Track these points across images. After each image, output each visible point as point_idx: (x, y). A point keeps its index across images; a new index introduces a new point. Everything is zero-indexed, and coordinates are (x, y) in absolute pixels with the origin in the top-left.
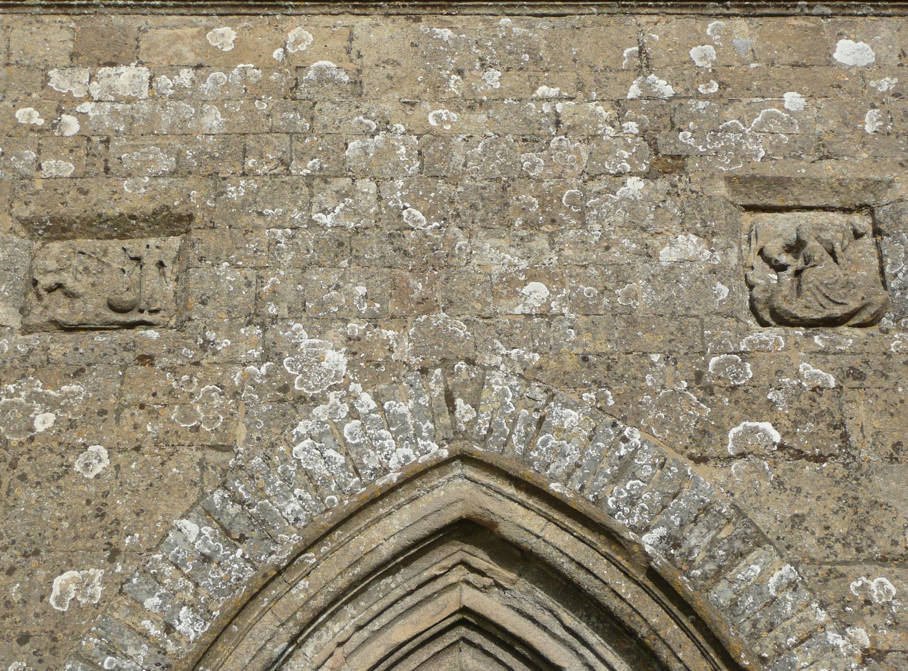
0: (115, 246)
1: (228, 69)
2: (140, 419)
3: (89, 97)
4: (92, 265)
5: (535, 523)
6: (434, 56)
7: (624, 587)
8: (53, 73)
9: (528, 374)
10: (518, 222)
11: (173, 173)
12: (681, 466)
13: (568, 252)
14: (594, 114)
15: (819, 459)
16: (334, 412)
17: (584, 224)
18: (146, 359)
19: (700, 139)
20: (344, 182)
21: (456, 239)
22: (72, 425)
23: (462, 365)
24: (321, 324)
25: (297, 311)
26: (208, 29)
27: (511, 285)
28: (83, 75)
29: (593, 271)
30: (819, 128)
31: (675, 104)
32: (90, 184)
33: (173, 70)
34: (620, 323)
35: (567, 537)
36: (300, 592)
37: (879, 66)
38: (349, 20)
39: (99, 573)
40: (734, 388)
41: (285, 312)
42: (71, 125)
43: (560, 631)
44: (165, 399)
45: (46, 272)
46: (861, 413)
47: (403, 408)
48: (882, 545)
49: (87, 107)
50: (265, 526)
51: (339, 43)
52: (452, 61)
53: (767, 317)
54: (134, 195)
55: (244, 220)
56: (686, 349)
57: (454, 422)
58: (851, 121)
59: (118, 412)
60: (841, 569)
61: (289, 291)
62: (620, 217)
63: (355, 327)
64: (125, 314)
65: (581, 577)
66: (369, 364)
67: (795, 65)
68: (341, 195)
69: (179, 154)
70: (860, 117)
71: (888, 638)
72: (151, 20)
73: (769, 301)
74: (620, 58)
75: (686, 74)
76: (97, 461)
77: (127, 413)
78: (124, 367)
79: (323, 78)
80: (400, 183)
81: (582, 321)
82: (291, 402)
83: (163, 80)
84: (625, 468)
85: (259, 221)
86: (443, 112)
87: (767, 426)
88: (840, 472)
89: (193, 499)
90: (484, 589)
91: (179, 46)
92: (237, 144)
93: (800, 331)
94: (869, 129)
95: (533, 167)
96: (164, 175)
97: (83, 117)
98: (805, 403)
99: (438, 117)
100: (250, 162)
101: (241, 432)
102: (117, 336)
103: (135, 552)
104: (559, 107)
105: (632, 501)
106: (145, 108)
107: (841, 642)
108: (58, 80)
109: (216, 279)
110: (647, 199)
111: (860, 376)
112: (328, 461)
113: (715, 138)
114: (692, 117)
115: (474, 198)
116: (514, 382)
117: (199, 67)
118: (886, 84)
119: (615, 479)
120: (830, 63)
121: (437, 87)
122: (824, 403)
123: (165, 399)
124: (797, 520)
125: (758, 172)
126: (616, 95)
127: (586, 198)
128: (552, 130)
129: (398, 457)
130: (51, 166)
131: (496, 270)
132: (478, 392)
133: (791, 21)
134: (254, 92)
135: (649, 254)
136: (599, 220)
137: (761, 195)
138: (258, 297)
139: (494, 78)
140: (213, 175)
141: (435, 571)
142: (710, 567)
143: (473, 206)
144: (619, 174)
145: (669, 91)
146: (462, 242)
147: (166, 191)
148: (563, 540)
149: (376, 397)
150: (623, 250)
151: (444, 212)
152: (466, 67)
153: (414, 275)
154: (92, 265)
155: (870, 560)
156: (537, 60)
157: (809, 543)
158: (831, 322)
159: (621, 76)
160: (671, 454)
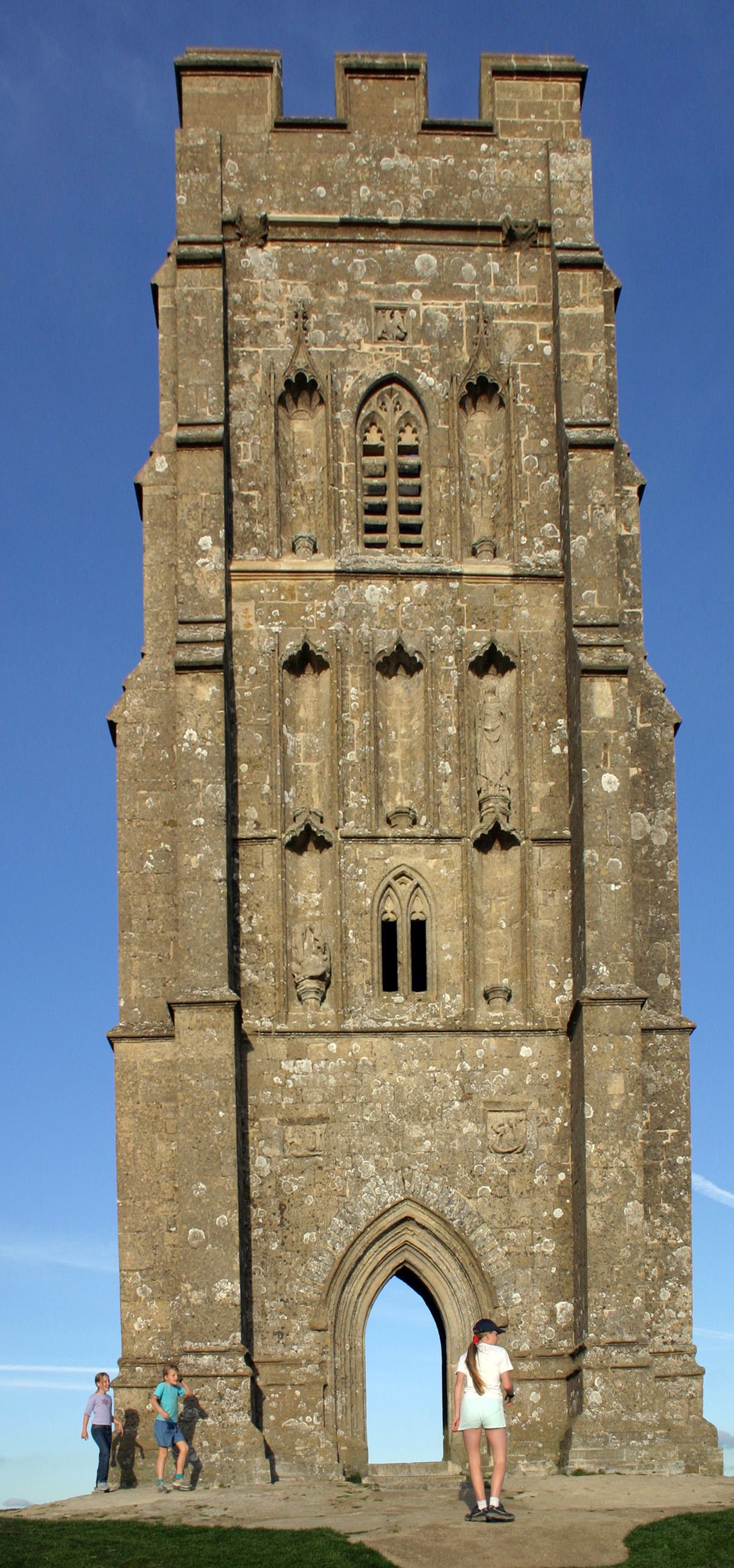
0: (307, 1128)
7: (448, 1236)
18: (320, 1168)
19: (477, 1087)
27: (420, 1141)
28: (292, 1062)
32: (298, 1106)
33: (318, 1061)
36: (367, 1238)
42: (291, 1085)
46: (513, 1183)
48: (514, 1223)
49: (294, 1076)
51: (368, 1050)
54: (311, 1111)
58: (522, 1079)
63: (377, 1157)
66: (382, 1171)
68: (372, 1109)
70: (525, 1078)
71: (512, 1249)
76: (310, 1200)
79: (364, 1064)
82: (360, 1181)
83: (316, 1065)
92: (340, 1090)
101: (348, 1191)
105: (451, 1211)
109: (338, 1141)
118: (534, 1064)
119: (447, 1205)
120: (518, 1056)
121: (399, 1067)
122: (504, 1180)
129: (390, 1199)
134: (344, 1069)
135: (459, 1130)
156: (429, 1055)
157: (495, 1223)
158: (510, 1152)
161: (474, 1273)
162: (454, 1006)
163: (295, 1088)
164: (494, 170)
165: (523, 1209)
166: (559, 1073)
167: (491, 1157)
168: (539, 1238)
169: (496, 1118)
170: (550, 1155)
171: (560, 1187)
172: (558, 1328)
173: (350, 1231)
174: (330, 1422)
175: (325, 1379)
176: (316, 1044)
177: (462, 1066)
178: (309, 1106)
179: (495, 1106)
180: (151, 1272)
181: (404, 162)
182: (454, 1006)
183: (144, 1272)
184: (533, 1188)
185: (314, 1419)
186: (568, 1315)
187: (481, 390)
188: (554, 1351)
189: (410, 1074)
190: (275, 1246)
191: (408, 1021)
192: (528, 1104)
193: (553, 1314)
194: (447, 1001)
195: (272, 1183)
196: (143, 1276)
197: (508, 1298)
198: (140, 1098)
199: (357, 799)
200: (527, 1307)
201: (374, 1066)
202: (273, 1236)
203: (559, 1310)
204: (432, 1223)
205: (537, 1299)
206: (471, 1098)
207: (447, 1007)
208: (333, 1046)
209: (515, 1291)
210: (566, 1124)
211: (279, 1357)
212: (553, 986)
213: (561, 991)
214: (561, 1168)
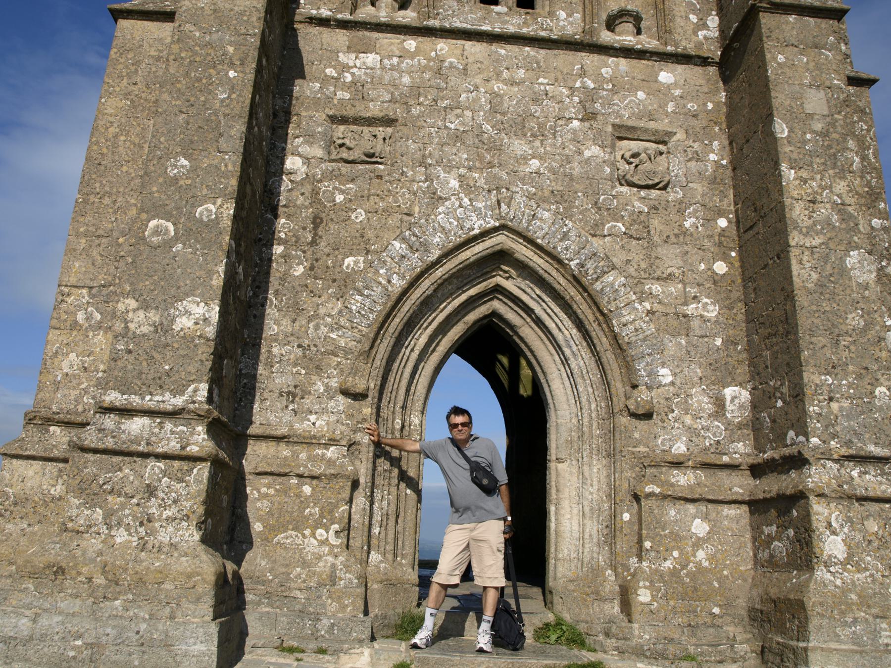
0: (366, 129)
1: (412, 59)
2: (377, 201)
3: (355, 66)
4: (357, 137)
5: (529, 254)
6: (497, 61)
7: (562, 281)
8: (340, 54)
9: (530, 197)
10: (529, 134)
11: (390, 101)
12: (586, 237)
13: (548, 148)
14: (561, 92)
15: (639, 239)
16: (453, 205)
17: (555, 138)
18: (380, 177)
20: (459, 111)
21: (503, 139)
22: (351, 201)
23: (504, 190)
24: (449, 169)
25: (439, 163)
26: (404, 41)
27: (525, 159)
28: (353, 56)
29: (557, 157)
30: (650, 108)
31: (594, 91)
33: (390, 57)
34: (567, 179)
35: (542, 260)
37: (676, 84)
38: (463, 42)
39: (362, 259)
40: (609, 209)
41: (434, 163)
42: (348, 78)
43: (534, 296)
44: (387, 194)
45: (339, 138)
46: (656, 223)
47: (480, 205)
48: (658, 273)
49: (355, 70)
50: (425, 247)
51: (459, 52)
52: (505, 64)
53: (623, 182)
54: (374, 109)
55: (419, 124)
56: (593, 192)
57: (500, 213)
58: (663, 106)
59: (368, 197)
60: (643, 281)
61: (436, 154)
62: (569, 136)
63: (462, 171)
64: (370, 157)
65: (546, 276)
66: (468, 187)
67: (643, 80)
68: (458, 116)
69: (392, 93)
70: (666, 105)
71: (657, 307)
72: (380, 35)
73: (624, 176)
74: (574, 70)
75: (598, 78)
76: (359, 216)
77: (372, 197)
78: (370, 179)
79: (452, 66)
80: (482, 113)
81: (552, 177)
82: (437, 199)
83: (386, 61)
84: (565, 237)
85: (425, 124)
86: (501, 85)
87: (620, 225)
88: (646, 244)
89: (398, 233)
90: (507, 279)
91: (392, 47)
92: (416, 90)
93: (635, 189)
94: (669, 110)
95: (536, 112)
96: (386, 102)
97: (353, 74)
98: (635, 217)
99: (498, 87)
100: (421, 99)
101: (417, 209)
102: (367, 166)
103: (376, 252)
104: (548, 88)
105: (567, 249)
106: (378, 72)
107: (640, 307)
108: (342, 57)
109: (407, 147)
110: (581, 130)
111: (657, 209)
112: (451, 223)
113: (609, 107)
114: (601, 98)
115: (511, 122)
116: (524, 199)
117: (400, 57)
118: (677, 92)
119: (561, 240)
120: (656, 81)
121: (498, 74)
122: (642, 218)
123: (387, 194)
124: (628, 261)
125: (625, 123)
126: (571, 85)
127: (556, 127)
128: (544, 97)
129: (477, 225)
130: (340, 94)
131: (519, 153)
132: (510, 202)
133: (643, 62)
135: (580, 153)
136: (561, 136)
137: (623, 133)
138: (424, 155)
139: (521, 73)
140: (406, 103)
141: (488, 269)
142: (595, 276)
143: (511, 126)
144: (570, 118)
145: (592, 86)
146: (506, 140)
147: (387, 108)
148: (540, 261)
149: (470, 200)
150: (570, 150)
151: (501, 128)
152: (510, 66)
153: (487, 152)
154: (357, 137)
155: (653, 278)
156: (539, 67)
157: (632, 270)
159: (573, 77)
160: (583, 232)
161: (601, 334)
162: (571, 23)
163: (354, 83)
165: (670, 259)
166: (710, 106)
167: (625, 189)
168: (695, 297)
169: (629, 146)
170: (703, 195)
171: (720, 235)
172: (728, 424)
173: (416, 262)
174: (357, 542)
175: (356, 472)
177: (583, 83)
178: (371, 104)
179: (623, 133)
180: (105, 291)
182: (571, 23)
183: (94, 291)
184: (685, 233)
185: (330, 535)
186: (741, 407)
188: (725, 459)
189: (513, 83)
190: (299, 270)
191: (512, 29)
192: (671, 134)
193: (720, 404)
195: (307, 189)
196: (92, 296)
197: (652, 374)
198: (139, 79)
200: (681, 390)
201: (465, 69)
202: (299, 257)
203: (728, 398)
204: (538, 262)
205: (696, 379)
206: (595, 119)
207: (561, 23)
208: (411, 43)
209: (663, 365)
210: (724, 162)
211: (284, 431)
212: (695, 21)
213: (705, 26)
214: (721, 214)
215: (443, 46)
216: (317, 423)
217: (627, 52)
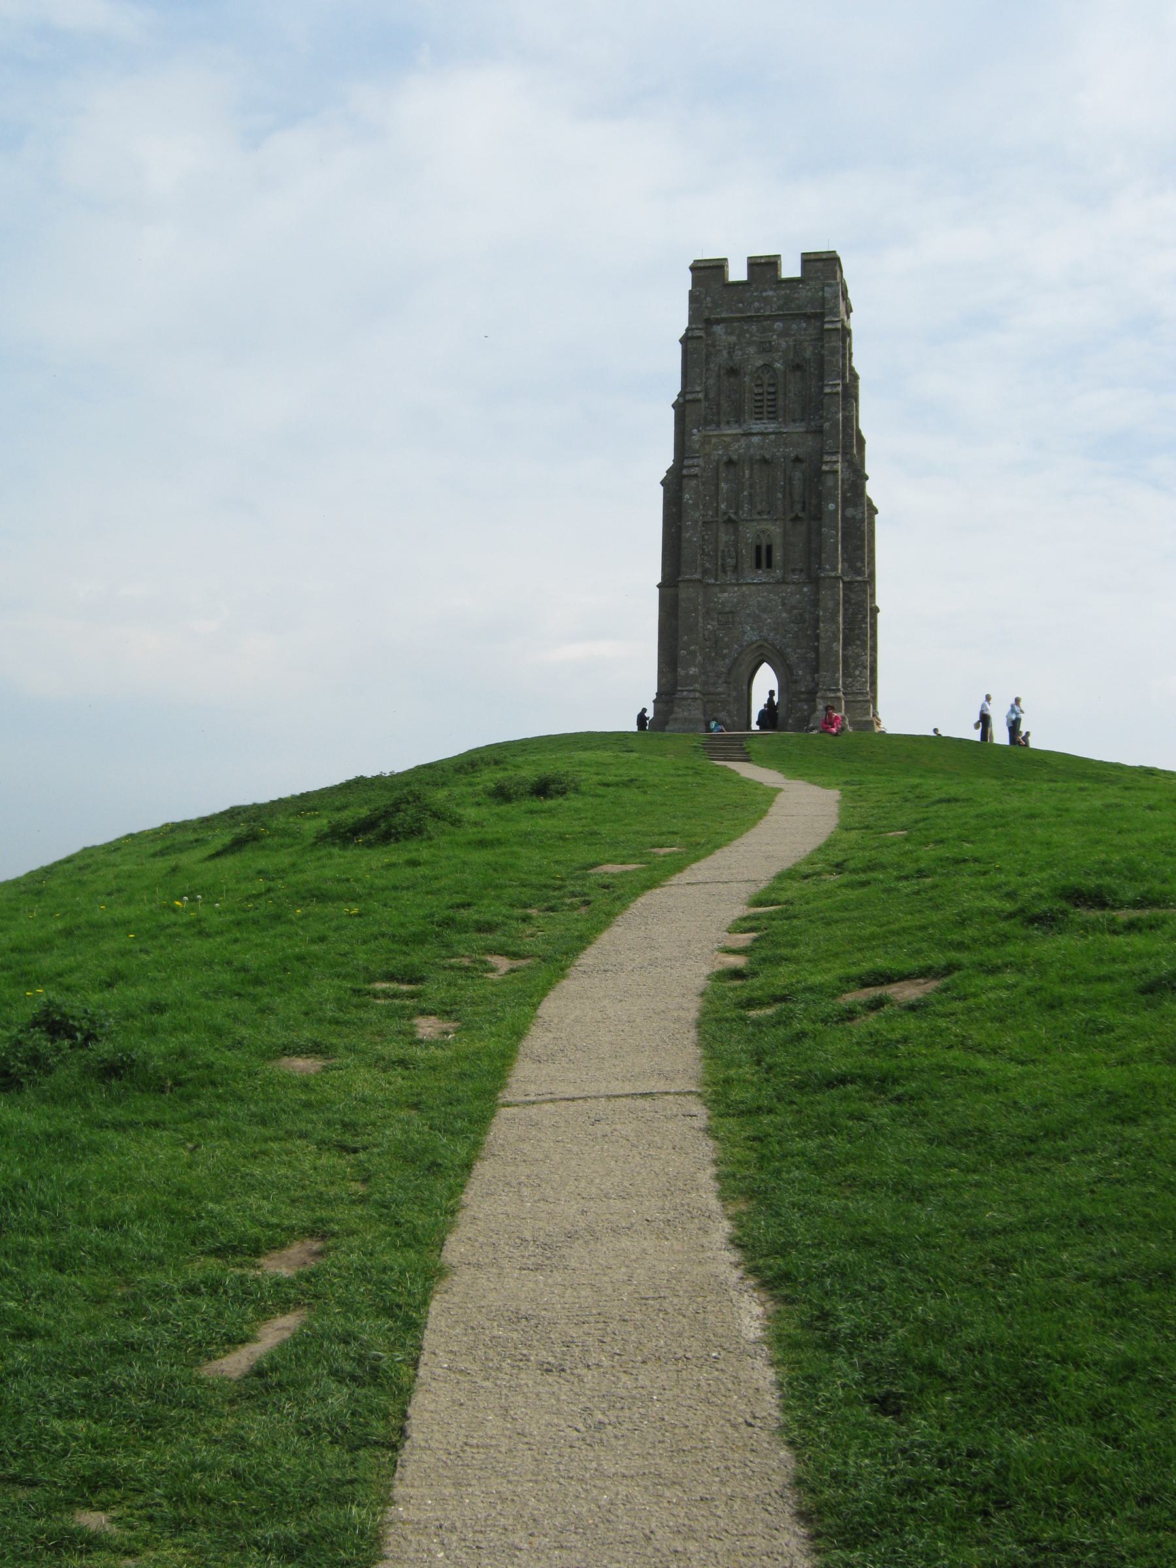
54: (727, 609)
164: (804, 293)
169: (795, 612)
176: (729, 588)
181: (771, 293)
187: (798, 367)
193: (813, 679)
194: (779, 573)
199: (746, 507)
215: (744, 588)
216: (720, 690)
217: (794, 583)
